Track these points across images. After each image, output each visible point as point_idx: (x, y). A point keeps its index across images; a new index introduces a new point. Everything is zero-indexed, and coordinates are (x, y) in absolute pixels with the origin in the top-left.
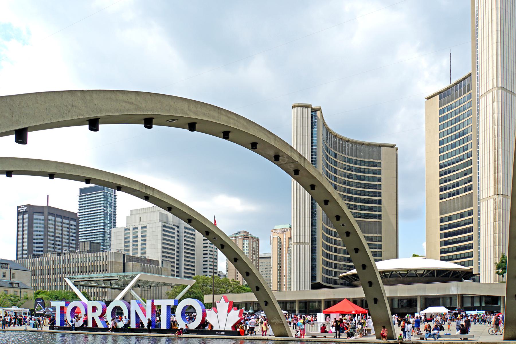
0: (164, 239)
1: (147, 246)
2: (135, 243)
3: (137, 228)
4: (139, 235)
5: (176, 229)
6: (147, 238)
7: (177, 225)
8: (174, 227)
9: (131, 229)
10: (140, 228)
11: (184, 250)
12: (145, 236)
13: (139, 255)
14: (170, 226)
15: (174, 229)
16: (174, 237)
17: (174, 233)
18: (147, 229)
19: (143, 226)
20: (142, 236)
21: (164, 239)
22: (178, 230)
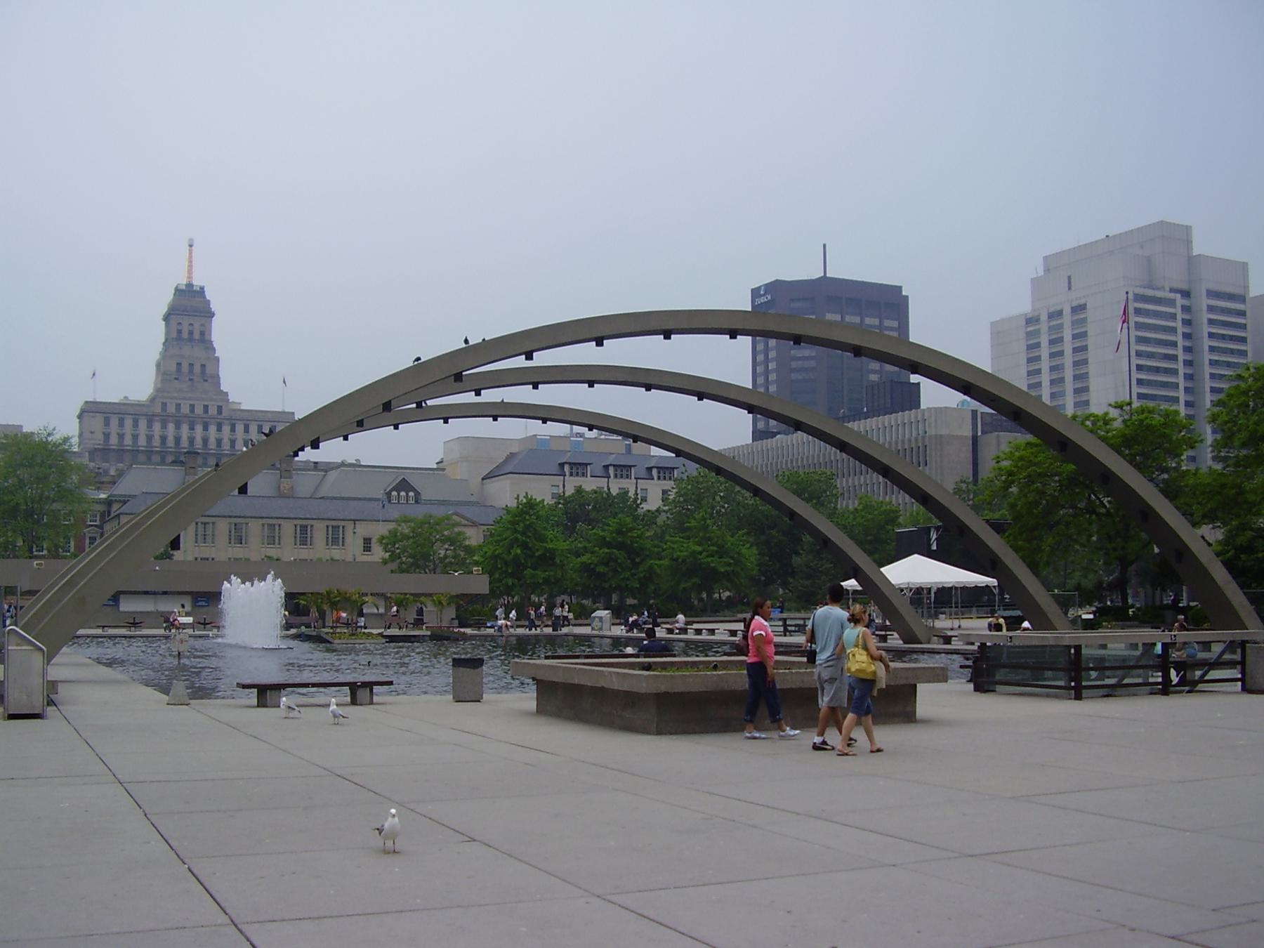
1: (1092, 369)
2: (1057, 362)
3: (1060, 313)
4: (1067, 334)
5: (1180, 301)
6: (1091, 342)
7: (1185, 287)
8: (1172, 296)
9: (1044, 317)
10: (1067, 311)
14: (1159, 294)
15: (1171, 303)
18: (1090, 314)
19: (1075, 304)
20: (1075, 337)
22: (1186, 302)
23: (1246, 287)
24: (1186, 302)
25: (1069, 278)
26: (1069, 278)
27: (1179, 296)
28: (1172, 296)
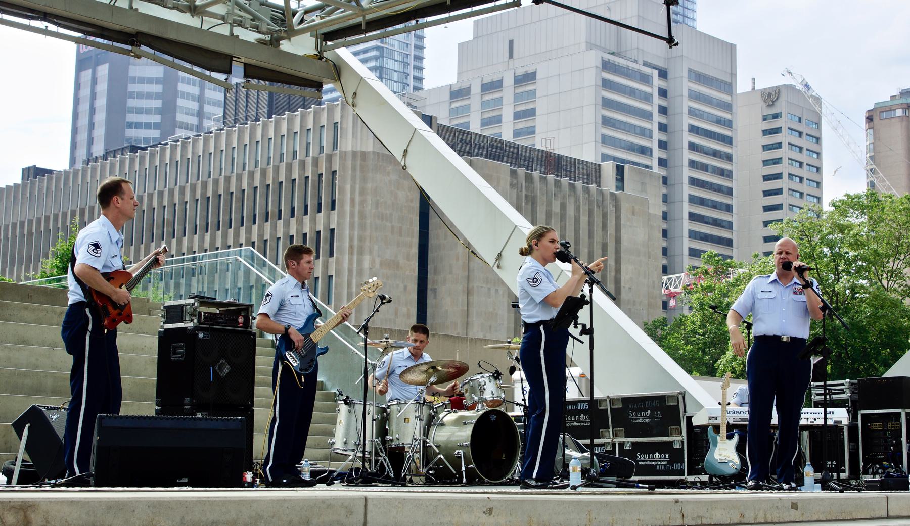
0: (606, 122)
3: (497, 85)
5: (657, 82)
7: (661, 64)
8: (647, 70)
9: (476, 89)
10: (509, 81)
11: (687, 173)
12: (531, 113)
13: (507, 136)
14: (632, 65)
15: (645, 79)
16: (648, 116)
17: (647, 98)
18: (539, 87)
20: (518, 116)
21: (607, 104)
23: (733, 75)
24: (663, 84)
25: (511, 43)
26: (511, 43)
27: (656, 73)
28: (647, 70)
